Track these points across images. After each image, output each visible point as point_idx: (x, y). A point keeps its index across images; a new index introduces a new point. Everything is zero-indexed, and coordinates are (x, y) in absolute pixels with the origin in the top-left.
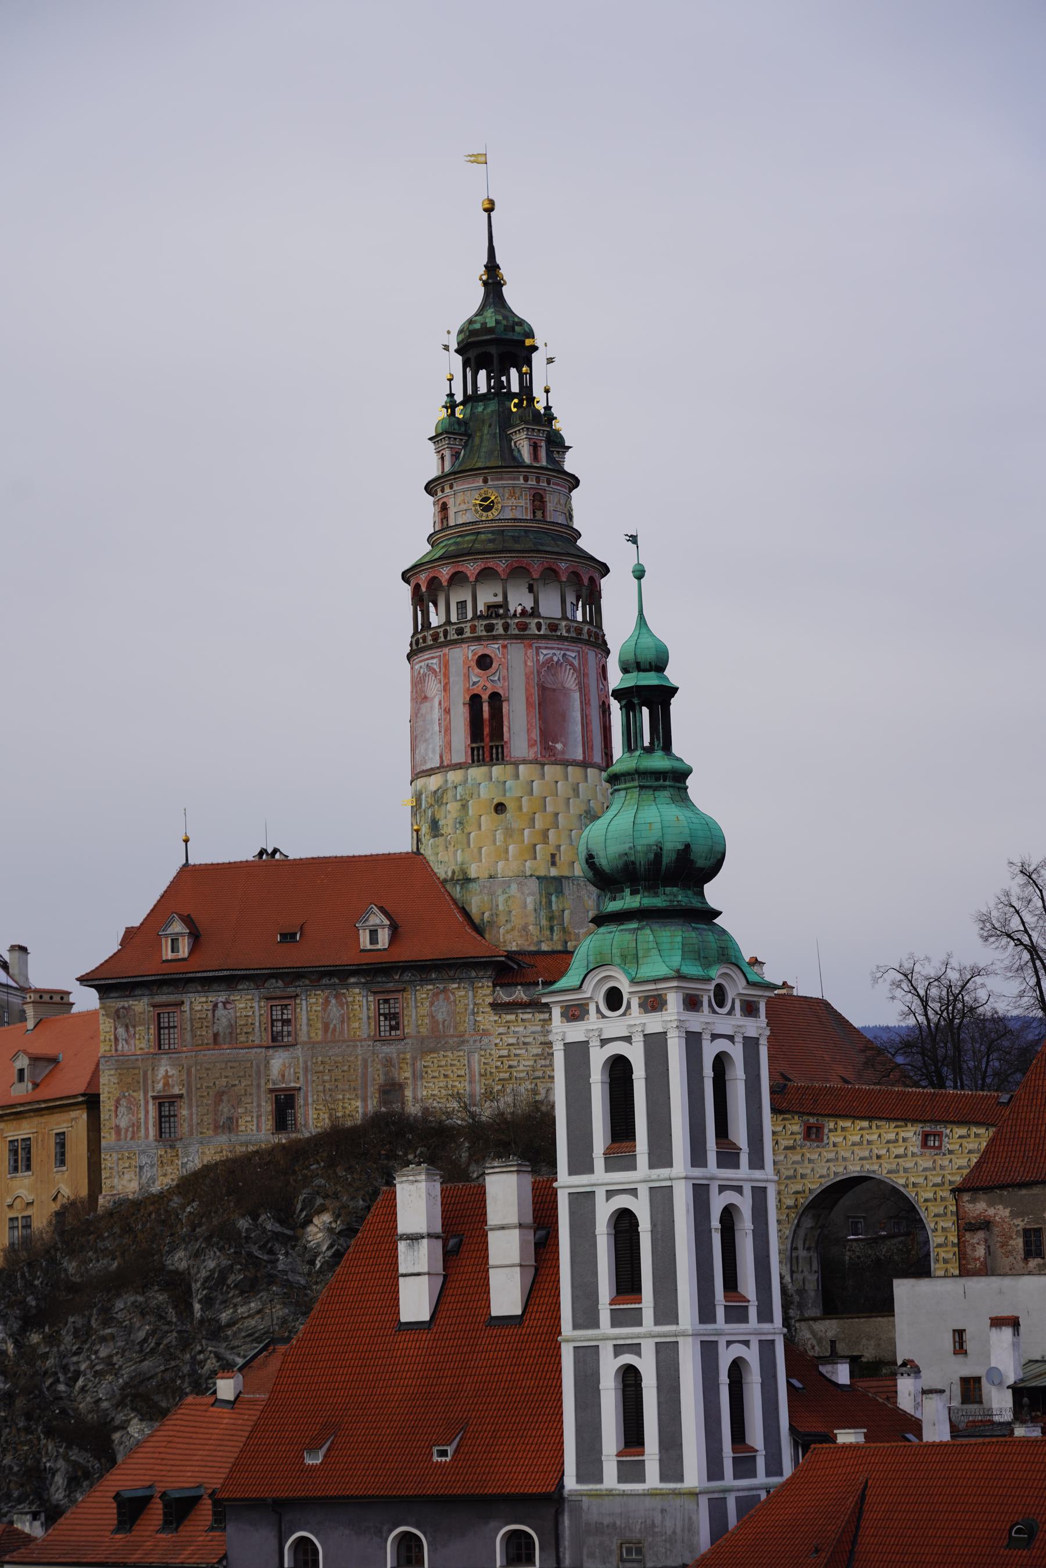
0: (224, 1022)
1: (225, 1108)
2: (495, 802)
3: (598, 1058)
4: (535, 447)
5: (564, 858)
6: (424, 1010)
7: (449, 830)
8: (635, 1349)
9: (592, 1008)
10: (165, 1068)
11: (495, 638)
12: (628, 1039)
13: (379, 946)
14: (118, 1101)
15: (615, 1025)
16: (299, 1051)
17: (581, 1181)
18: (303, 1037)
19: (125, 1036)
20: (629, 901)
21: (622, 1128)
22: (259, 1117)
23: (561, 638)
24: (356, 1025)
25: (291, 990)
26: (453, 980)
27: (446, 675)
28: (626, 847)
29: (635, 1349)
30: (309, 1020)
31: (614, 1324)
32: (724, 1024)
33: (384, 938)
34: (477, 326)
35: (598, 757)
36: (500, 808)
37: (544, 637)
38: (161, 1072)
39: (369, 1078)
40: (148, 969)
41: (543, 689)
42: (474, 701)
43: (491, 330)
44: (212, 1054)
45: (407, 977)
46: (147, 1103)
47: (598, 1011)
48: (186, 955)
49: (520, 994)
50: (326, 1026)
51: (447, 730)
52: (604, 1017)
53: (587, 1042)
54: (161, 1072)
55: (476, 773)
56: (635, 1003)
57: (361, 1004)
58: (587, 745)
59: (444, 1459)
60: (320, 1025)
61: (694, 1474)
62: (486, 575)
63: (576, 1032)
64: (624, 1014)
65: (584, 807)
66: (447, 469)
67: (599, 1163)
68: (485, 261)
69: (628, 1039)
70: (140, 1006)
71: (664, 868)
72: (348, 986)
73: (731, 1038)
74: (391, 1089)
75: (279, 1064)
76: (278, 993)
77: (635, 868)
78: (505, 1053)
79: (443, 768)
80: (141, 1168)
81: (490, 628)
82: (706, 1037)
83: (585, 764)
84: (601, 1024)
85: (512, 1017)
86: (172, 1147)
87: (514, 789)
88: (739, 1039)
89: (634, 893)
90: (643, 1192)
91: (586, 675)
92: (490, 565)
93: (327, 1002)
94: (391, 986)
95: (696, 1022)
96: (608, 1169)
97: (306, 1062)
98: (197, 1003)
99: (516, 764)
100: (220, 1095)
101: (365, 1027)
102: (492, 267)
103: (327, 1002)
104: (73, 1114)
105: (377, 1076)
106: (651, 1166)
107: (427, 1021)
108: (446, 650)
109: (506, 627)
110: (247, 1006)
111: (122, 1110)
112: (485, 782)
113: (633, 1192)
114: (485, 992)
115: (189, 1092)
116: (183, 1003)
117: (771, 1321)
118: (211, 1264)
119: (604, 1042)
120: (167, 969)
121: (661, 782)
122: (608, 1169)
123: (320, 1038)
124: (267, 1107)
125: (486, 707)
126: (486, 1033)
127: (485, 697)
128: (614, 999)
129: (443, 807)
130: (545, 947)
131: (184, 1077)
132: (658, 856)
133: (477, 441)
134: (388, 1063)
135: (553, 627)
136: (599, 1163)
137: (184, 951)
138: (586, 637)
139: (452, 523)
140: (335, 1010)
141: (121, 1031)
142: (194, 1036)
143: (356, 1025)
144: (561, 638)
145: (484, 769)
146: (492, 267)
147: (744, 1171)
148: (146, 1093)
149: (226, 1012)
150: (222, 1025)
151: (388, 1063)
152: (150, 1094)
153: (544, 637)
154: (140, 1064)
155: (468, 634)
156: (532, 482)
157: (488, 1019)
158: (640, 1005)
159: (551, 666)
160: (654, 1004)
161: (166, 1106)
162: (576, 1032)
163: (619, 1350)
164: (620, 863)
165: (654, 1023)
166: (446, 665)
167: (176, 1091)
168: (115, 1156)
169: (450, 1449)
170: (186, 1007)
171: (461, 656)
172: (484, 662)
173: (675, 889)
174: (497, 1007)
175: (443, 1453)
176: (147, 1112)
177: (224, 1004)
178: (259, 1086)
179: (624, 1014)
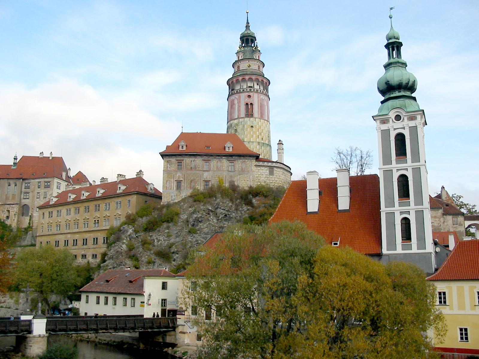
0: (193, 165)
1: (193, 184)
2: (251, 125)
5: (264, 139)
6: (240, 165)
7: (240, 131)
8: (408, 213)
9: (391, 120)
10: (179, 174)
11: (252, 92)
12: (404, 128)
13: (230, 151)
14: (167, 181)
15: (398, 124)
16: (211, 172)
18: (212, 169)
19: (169, 166)
22: (201, 186)
24: (224, 167)
25: (209, 159)
26: (247, 159)
27: (240, 99)
28: (400, 78)
29: (408, 213)
30: (213, 166)
33: (231, 150)
34: (246, 33)
37: (261, 93)
38: (178, 175)
39: (227, 179)
40: (176, 152)
42: (247, 104)
43: (249, 34)
44: (190, 172)
45: (236, 158)
46: (174, 182)
48: (185, 149)
49: (261, 163)
50: (217, 167)
51: (239, 110)
52: (395, 122)
54: (178, 175)
55: (247, 119)
56: (406, 118)
59: (336, 246)
60: (216, 167)
61: (430, 248)
62: (251, 80)
63: (384, 127)
64: (402, 121)
66: (242, 58)
67: (394, 162)
70: (173, 160)
71: (409, 86)
72: (222, 158)
76: (206, 159)
77: (402, 84)
78: (258, 176)
79: (238, 118)
80: (172, 196)
84: (394, 124)
85: (260, 168)
86: (179, 192)
89: (399, 92)
90: (410, 170)
92: (251, 77)
93: (217, 162)
94: (232, 160)
96: (397, 163)
97: (212, 175)
98: (187, 160)
99: (256, 118)
100: (191, 181)
101: (226, 168)
102: (248, 23)
103: (217, 162)
104: (133, 196)
105: (228, 179)
107: (240, 168)
108: (240, 94)
109: (254, 90)
110: (199, 161)
111: (168, 183)
112: (249, 121)
114: (254, 162)
115: (184, 180)
116: (183, 160)
118: (195, 216)
119: (395, 129)
120: (180, 152)
121: (403, 66)
122: (397, 163)
123: (215, 170)
125: (249, 106)
127: (249, 104)
129: (238, 126)
131: (183, 176)
132: (409, 82)
133: (246, 54)
134: (231, 176)
136: (394, 162)
137: (185, 148)
139: (241, 69)
140: (219, 164)
141: (168, 165)
142: (186, 168)
143: (224, 167)
145: (248, 119)
146: (248, 23)
148: (174, 179)
149: (194, 163)
150: (193, 166)
152: (175, 180)
153: (261, 93)
154: (173, 173)
155: (245, 90)
156: (258, 63)
157: (254, 168)
160: (412, 118)
161: (179, 182)
162: (384, 127)
163: (401, 213)
164: (398, 83)
165: (412, 124)
166: (240, 97)
167: (181, 179)
168: (166, 193)
169: (338, 243)
170: (185, 160)
171: (243, 96)
172: (249, 96)
173: (409, 93)
174: (256, 166)
175: (336, 244)
176: (174, 184)
177: (194, 161)
178: (201, 179)
179: (402, 121)
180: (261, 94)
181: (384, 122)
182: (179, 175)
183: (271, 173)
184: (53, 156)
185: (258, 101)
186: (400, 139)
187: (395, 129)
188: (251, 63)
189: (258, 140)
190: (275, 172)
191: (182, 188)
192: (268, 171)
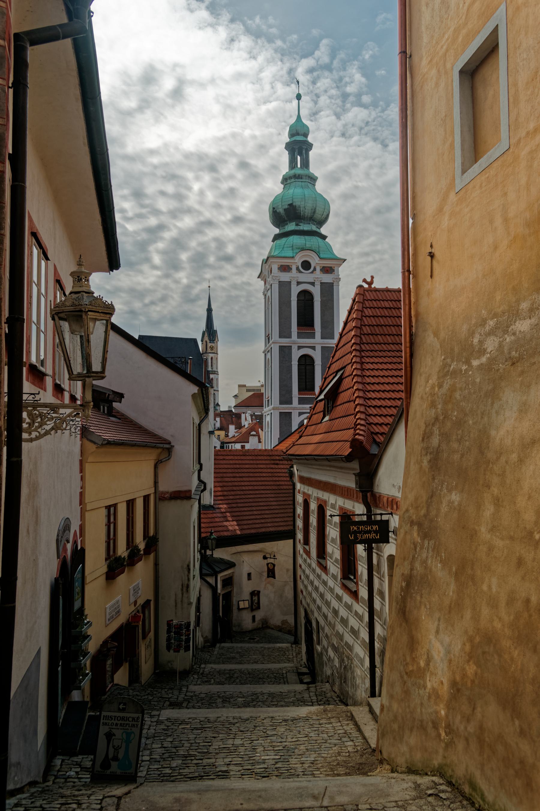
3: (295, 290)
12: (313, 284)
15: (306, 276)
17: (285, 342)
21: (306, 321)
31: (300, 403)
47: (298, 269)
52: (300, 272)
53: (291, 282)
56: (318, 269)
63: (285, 277)
64: (312, 272)
69: (313, 284)
84: (299, 275)
106: (322, 338)
113: (313, 348)
119: (299, 283)
128: (306, 265)
158: (321, 270)
179: (312, 272)
181: (285, 268)
186: (306, 298)
187: (299, 283)
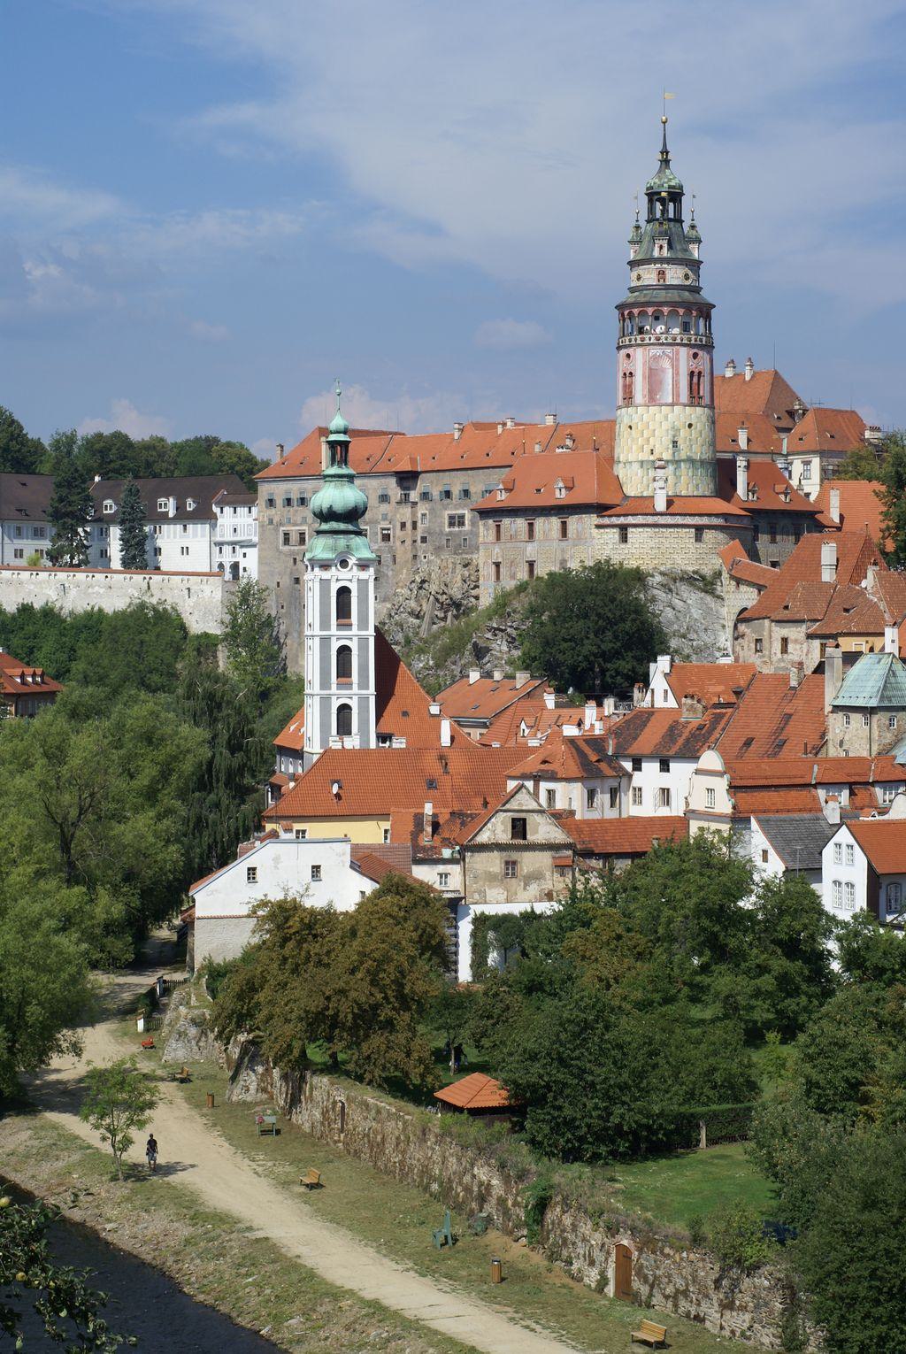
4: (661, 247)
5: (656, 452)
11: (631, 346)
16: (535, 544)
20: (325, 527)
23: (663, 344)
32: (344, 574)
35: (684, 397)
36: (630, 427)
41: (650, 369)
49: (606, 521)
57: (555, 522)
58: (676, 393)
65: (670, 426)
68: (660, 147)
72: (551, 515)
73: (350, 580)
74: (563, 562)
75: (531, 550)
81: (630, 341)
82: (334, 579)
83: (672, 405)
87: (636, 419)
88: (355, 580)
91: (678, 360)
95: (326, 575)
98: (506, 522)
102: (665, 152)
110: (521, 523)
114: (593, 519)
117: (367, 688)
124: (526, 567)
126: (594, 538)
130: (645, 495)
135: (658, 339)
138: (678, 341)
144: (663, 344)
146: (665, 152)
147: (355, 630)
151: (563, 551)
157: (595, 531)
159: (656, 358)
174: (598, 527)
180: (652, 347)
182: (497, 553)
183: (624, 539)
184: (756, 368)
185: (644, 364)
188: (641, 270)
189: (641, 457)
190: (629, 536)
191: (501, 577)
192: (617, 536)
